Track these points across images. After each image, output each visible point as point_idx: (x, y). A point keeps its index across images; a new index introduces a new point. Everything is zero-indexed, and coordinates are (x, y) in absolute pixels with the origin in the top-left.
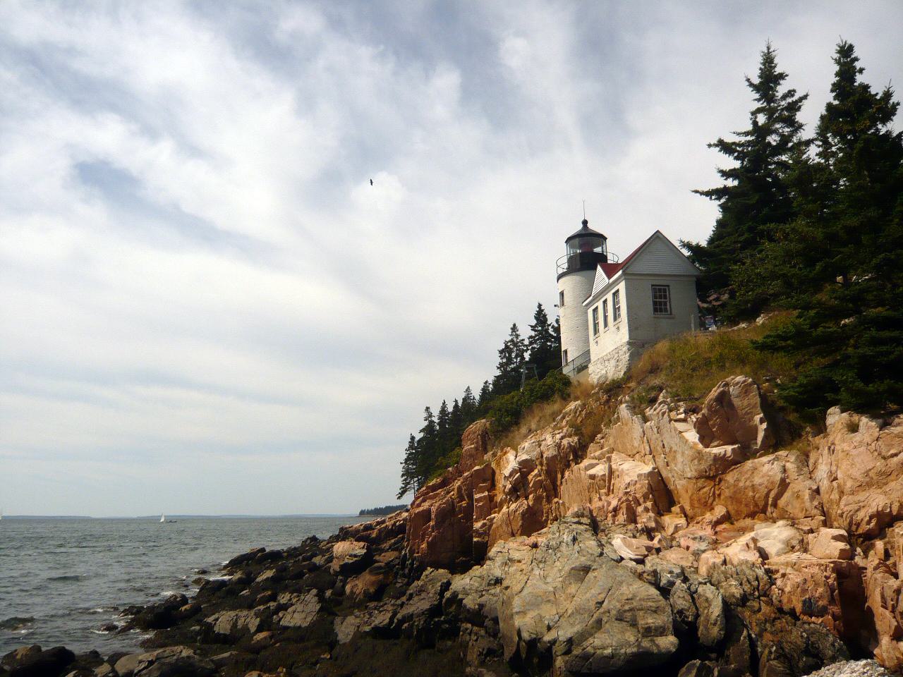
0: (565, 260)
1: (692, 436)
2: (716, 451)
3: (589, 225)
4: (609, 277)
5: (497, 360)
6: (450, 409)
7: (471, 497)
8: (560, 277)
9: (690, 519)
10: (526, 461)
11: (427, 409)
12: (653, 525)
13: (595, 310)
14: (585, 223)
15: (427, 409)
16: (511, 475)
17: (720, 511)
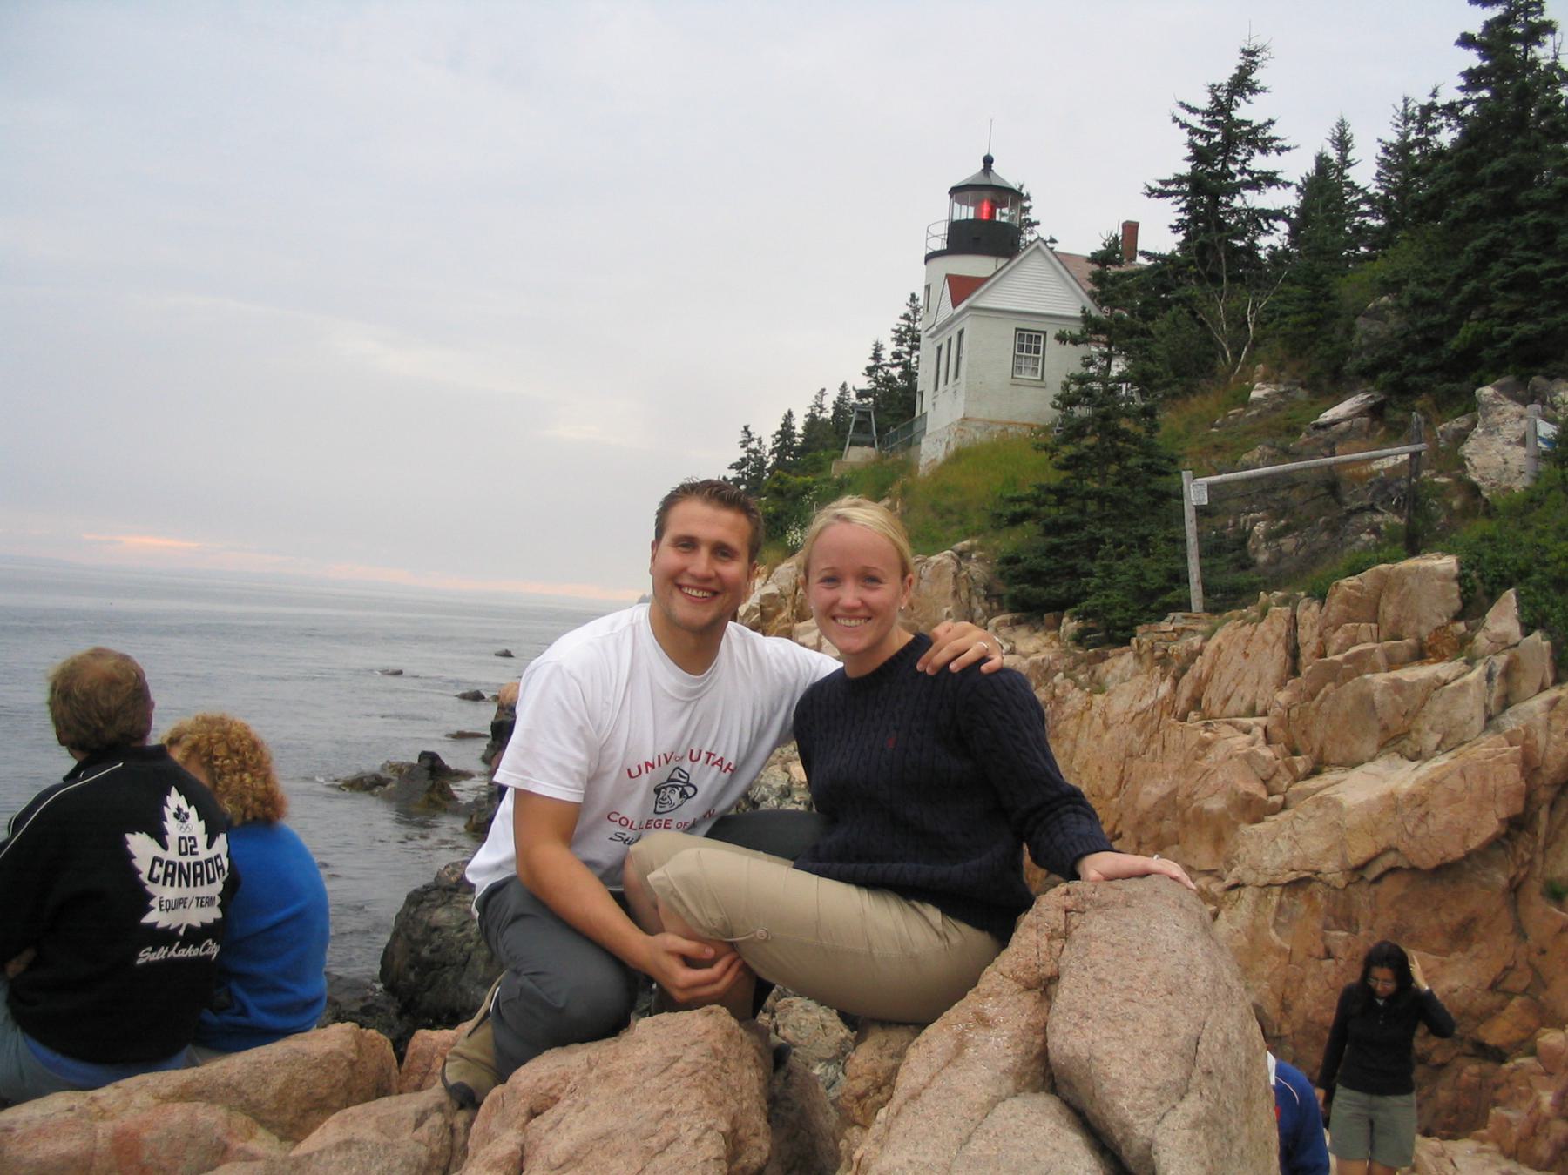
0: (942, 229)
3: (994, 166)
4: (955, 305)
6: (799, 426)
8: (929, 258)
10: (771, 596)
11: (746, 428)
13: (940, 349)
14: (988, 161)
15: (746, 428)
16: (747, 614)
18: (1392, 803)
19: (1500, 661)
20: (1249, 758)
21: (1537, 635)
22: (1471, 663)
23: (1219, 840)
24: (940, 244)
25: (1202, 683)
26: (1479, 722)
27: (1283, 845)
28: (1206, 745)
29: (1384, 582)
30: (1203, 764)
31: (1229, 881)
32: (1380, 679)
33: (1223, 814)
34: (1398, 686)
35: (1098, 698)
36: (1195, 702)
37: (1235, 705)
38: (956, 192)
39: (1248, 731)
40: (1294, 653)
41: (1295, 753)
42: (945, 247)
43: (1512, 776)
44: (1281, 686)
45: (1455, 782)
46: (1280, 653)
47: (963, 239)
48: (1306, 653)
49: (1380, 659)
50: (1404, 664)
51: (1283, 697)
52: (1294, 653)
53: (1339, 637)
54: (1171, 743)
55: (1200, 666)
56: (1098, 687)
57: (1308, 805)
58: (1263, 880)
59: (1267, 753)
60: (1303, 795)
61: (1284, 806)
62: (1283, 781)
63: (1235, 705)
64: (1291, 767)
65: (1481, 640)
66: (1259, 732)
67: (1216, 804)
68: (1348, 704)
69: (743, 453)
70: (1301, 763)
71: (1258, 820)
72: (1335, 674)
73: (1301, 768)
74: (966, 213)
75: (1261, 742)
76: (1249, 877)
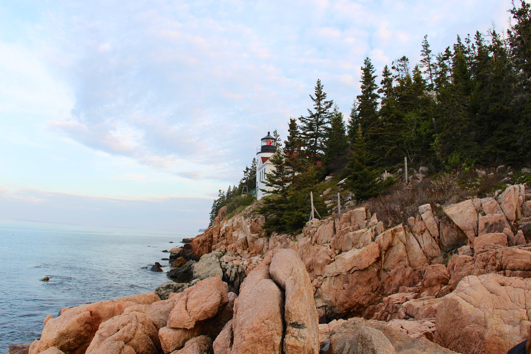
0: (260, 148)
1: (250, 231)
2: (253, 235)
4: (263, 163)
5: (242, 175)
6: (231, 190)
7: (212, 236)
9: (249, 252)
12: (240, 253)
17: (254, 251)
18: (355, 258)
19: (374, 228)
20: (327, 252)
21: (380, 222)
22: (368, 228)
23: (322, 269)
24: (260, 151)
25: (317, 237)
26: (370, 240)
27: (334, 268)
28: (318, 250)
29: (351, 214)
30: (318, 254)
31: (324, 276)
32: (351, 233)
33: (322, 264)
34: (355, 234)
35: (296, 242)
36: (316, 242)
37: (323, 242)
38: (262, 139)
39: (326, 246)
40: (335, 230)
41: (336, 249)
42: (260, 151)
43: (377, 250)
44: (332, 237)
45: (366, 252)
46: (332, 230)
47: (265, 149)
48: (337, 229)
49: (351, 229)
50: (356, 230)
51: (333, 239)
52: (335, 230)
53: (343, 226)
54: (311, 250)
55: (317, 234)
56: (296, 241)
57: (339, 260)
58: (331, 276)
59: (330, 250)
60: (337, 258)
61: (334, 261)
62: (333, 256)
63: (323, 242)
64: (335, 253)
65: (370, 224)
66: (328, 246)
67: (321, 262)
68: (345, 238)
69: (220, 197)
70: (337, 252)
71: (329, 264)
72: (343, 233)
73: (337, 253)
74: (265, 144)
75: (329, 248)
76: (328, 275)
